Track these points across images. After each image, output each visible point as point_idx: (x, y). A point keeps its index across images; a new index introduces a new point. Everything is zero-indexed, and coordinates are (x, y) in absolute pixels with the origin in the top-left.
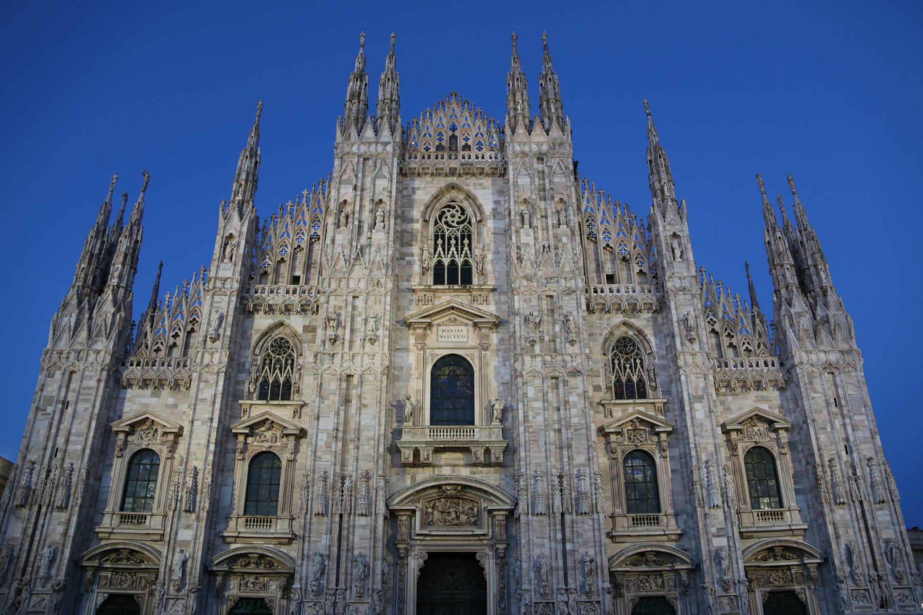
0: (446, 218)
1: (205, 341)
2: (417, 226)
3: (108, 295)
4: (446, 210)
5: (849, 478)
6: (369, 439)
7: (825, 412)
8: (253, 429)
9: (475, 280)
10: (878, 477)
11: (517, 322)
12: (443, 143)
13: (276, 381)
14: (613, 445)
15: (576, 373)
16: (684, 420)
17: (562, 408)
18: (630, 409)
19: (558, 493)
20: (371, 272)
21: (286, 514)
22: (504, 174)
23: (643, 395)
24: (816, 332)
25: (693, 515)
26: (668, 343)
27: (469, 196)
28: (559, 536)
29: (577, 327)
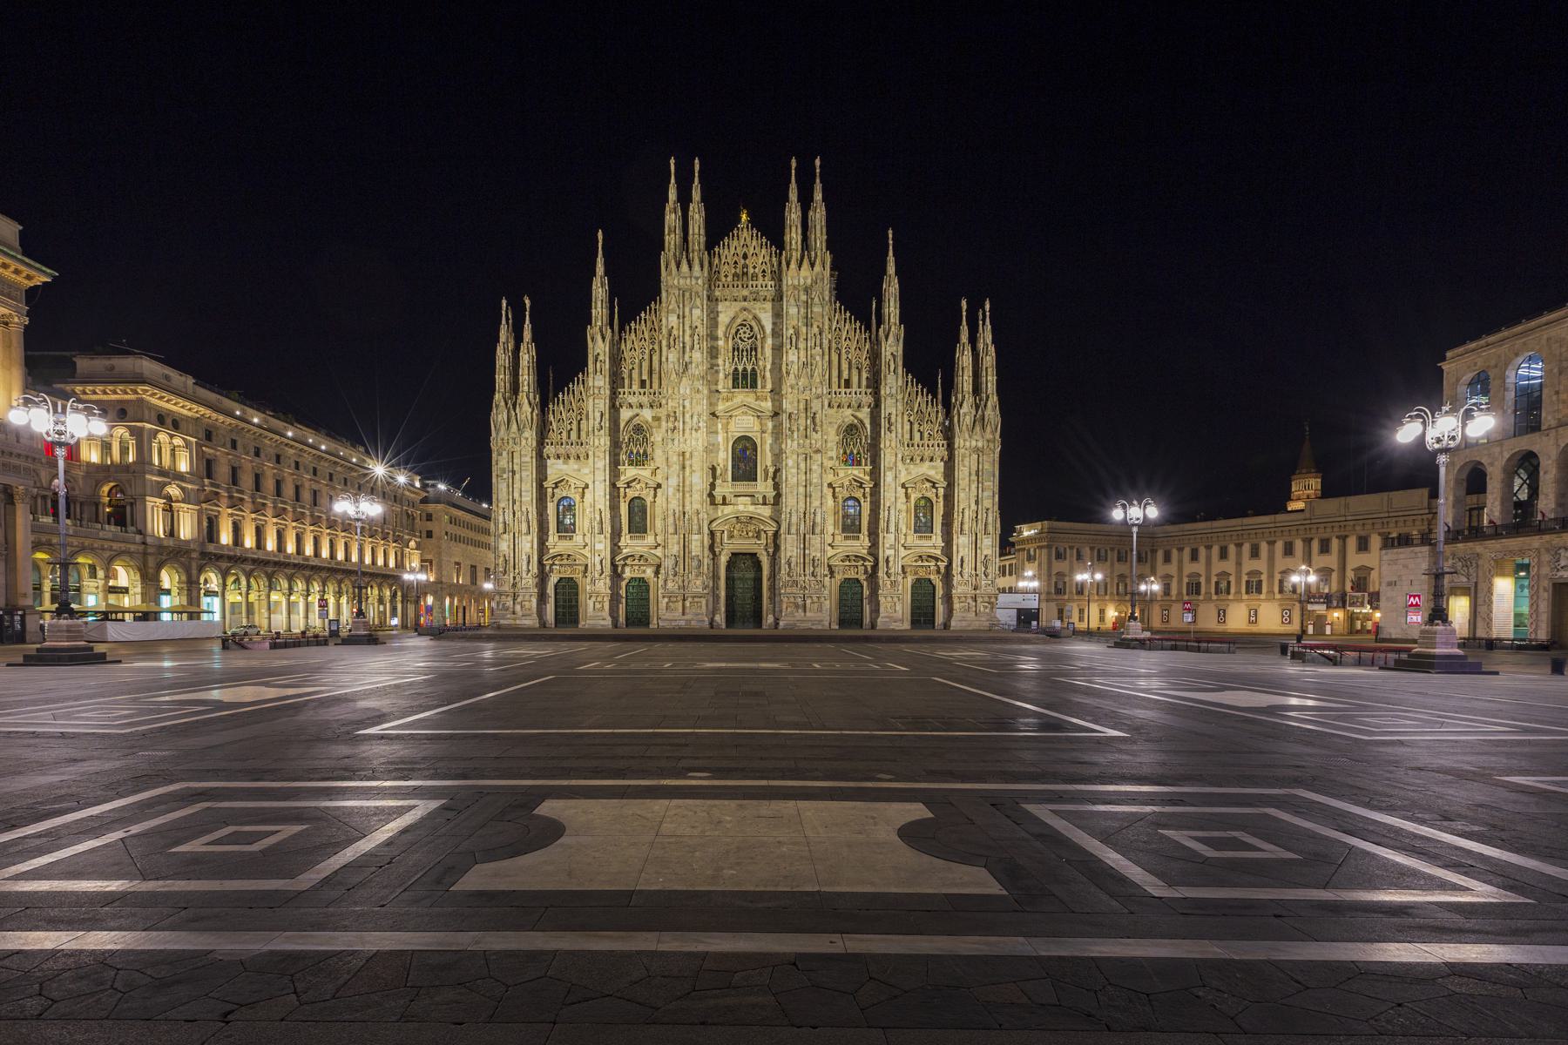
3: (523, 398)
8: (628, 485)
10: (990, 519)
15: (818, 451)
23: (859, 464)
27: (755, 317)
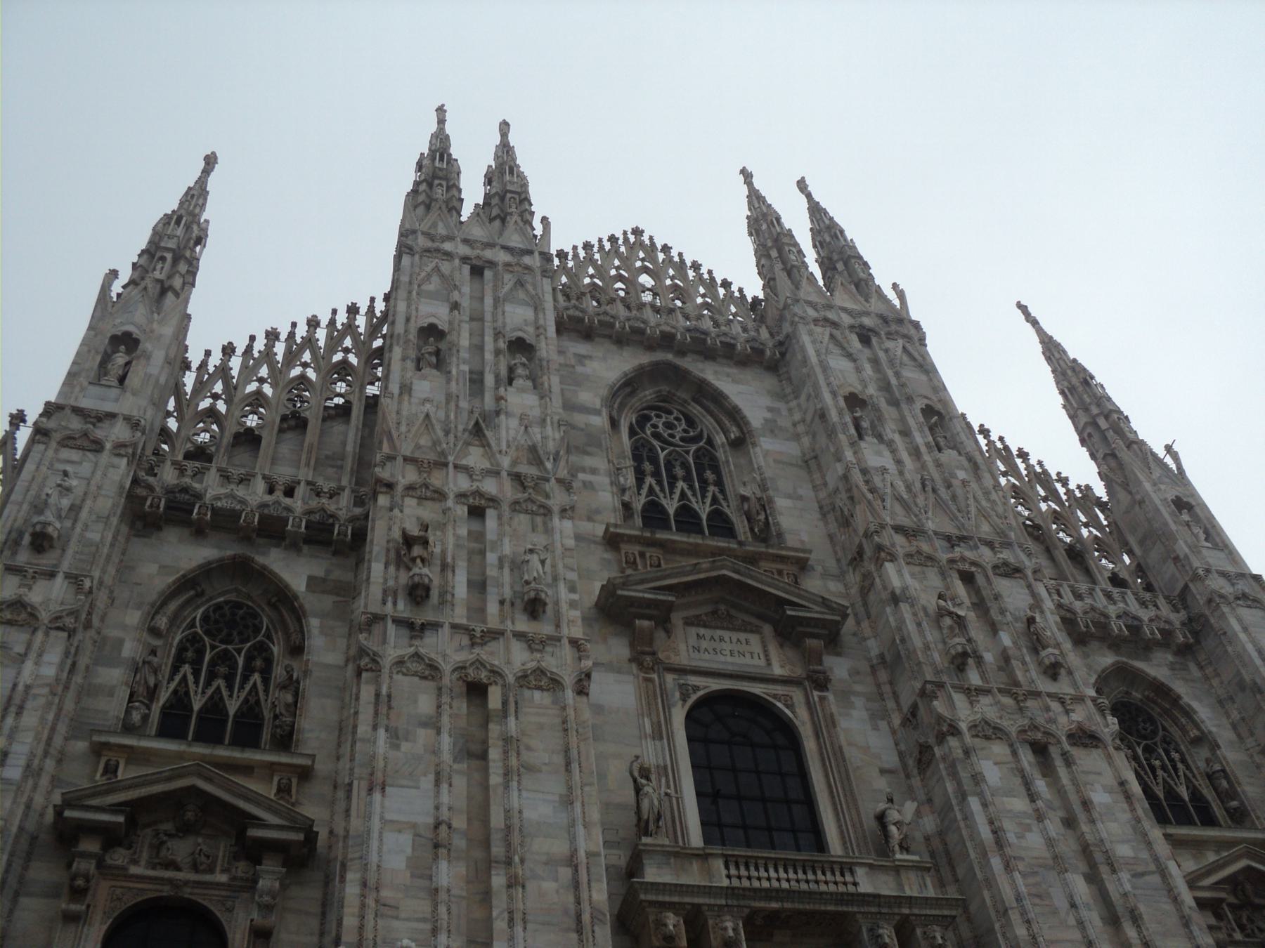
0: (655, 426)
1: (17, 543)
2: (600, 421)
4: (653, 414)
6: (550, 862)
11: (908, 617)
13: (215, 706)
15: (1085, 738)
17: (1082, 817)
20: (515, 463)
26: (1235, 715)
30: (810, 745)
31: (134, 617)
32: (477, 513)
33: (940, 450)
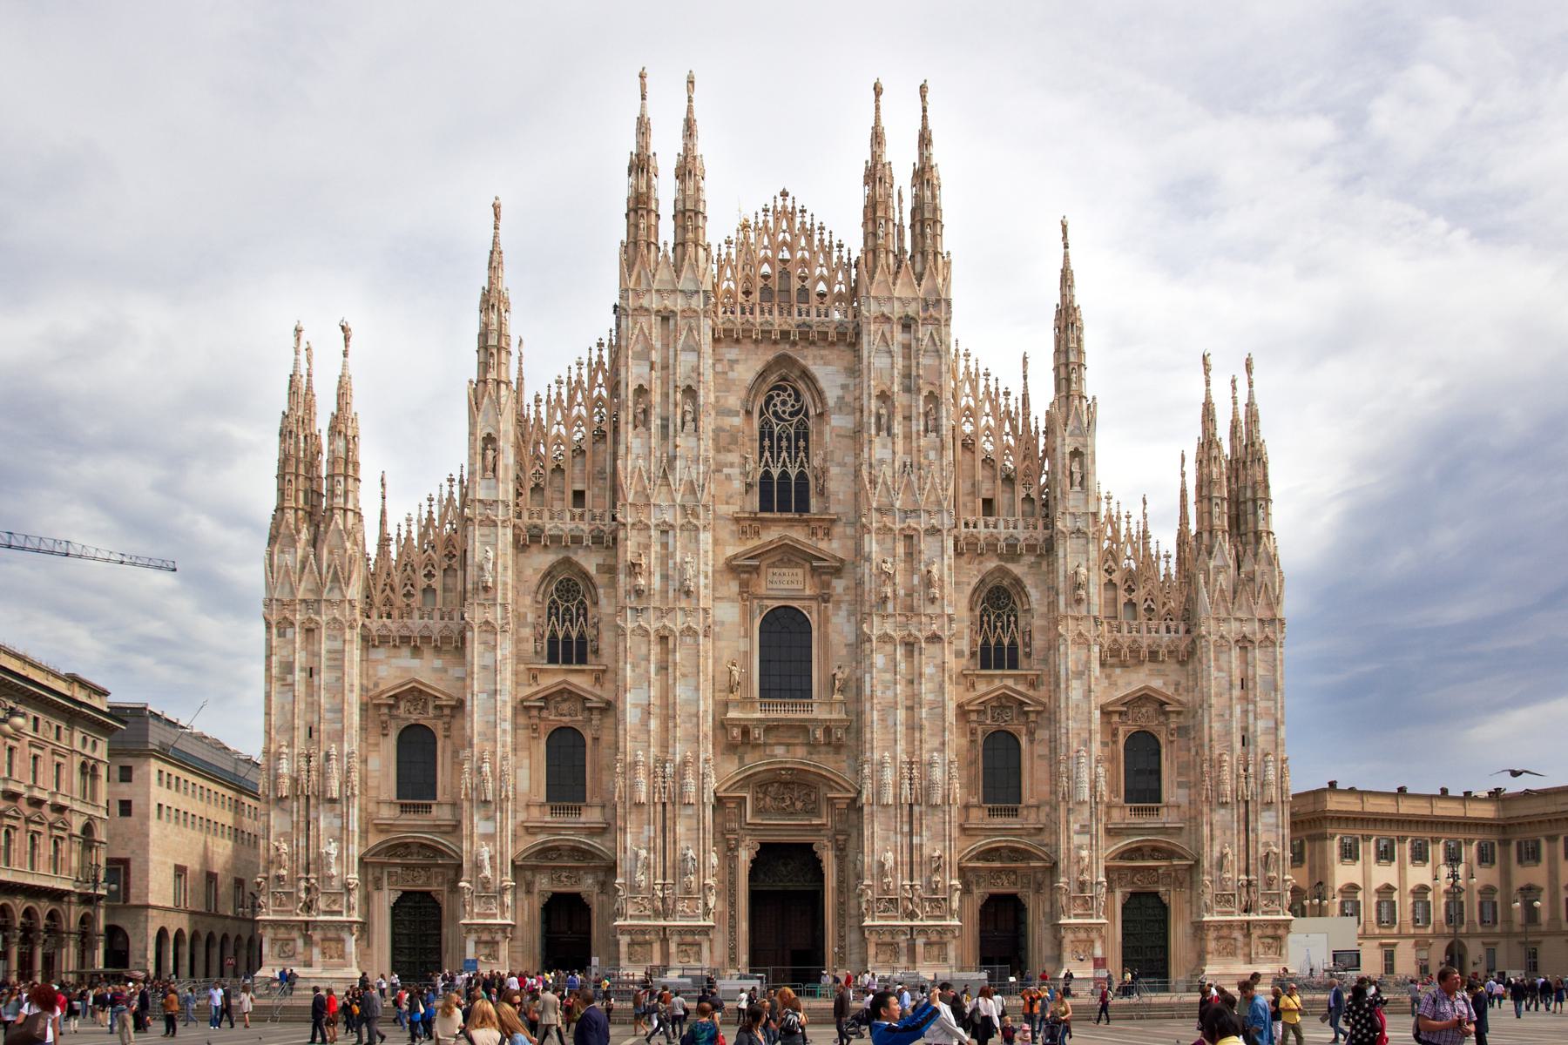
2: (737, 421)
4: (774, 393)
5: (1238, 776)
6: (690, 716)
7: (1227, 696)
9: (813, 502)
12: (770, 283)
13: (567, 636)
14: (974, 725)
15: (935, 639)
16: (1057, 700)
18: (997, 683)
19: (907, 782)
21: (596, 800)
22: (854, 345)
23: (1014, 664)
24: (1235, 592)
25: (1055, 808)
28: (906, 828)
29: (941, 579)
30: (815, 634)
31: (528, 600)
32: (665, 532)
33: (926, 430)
